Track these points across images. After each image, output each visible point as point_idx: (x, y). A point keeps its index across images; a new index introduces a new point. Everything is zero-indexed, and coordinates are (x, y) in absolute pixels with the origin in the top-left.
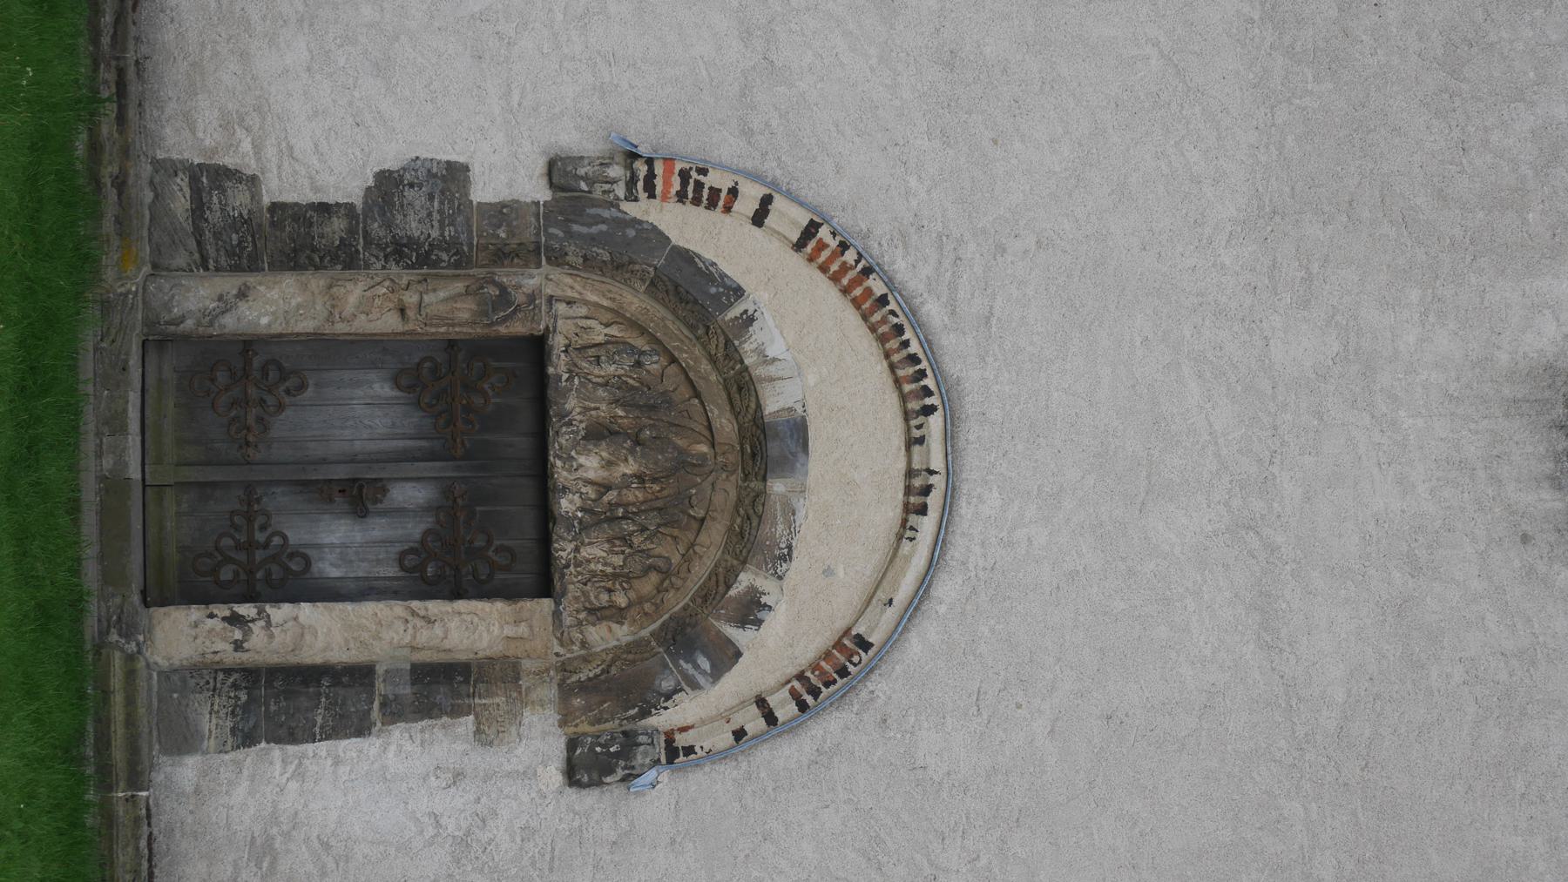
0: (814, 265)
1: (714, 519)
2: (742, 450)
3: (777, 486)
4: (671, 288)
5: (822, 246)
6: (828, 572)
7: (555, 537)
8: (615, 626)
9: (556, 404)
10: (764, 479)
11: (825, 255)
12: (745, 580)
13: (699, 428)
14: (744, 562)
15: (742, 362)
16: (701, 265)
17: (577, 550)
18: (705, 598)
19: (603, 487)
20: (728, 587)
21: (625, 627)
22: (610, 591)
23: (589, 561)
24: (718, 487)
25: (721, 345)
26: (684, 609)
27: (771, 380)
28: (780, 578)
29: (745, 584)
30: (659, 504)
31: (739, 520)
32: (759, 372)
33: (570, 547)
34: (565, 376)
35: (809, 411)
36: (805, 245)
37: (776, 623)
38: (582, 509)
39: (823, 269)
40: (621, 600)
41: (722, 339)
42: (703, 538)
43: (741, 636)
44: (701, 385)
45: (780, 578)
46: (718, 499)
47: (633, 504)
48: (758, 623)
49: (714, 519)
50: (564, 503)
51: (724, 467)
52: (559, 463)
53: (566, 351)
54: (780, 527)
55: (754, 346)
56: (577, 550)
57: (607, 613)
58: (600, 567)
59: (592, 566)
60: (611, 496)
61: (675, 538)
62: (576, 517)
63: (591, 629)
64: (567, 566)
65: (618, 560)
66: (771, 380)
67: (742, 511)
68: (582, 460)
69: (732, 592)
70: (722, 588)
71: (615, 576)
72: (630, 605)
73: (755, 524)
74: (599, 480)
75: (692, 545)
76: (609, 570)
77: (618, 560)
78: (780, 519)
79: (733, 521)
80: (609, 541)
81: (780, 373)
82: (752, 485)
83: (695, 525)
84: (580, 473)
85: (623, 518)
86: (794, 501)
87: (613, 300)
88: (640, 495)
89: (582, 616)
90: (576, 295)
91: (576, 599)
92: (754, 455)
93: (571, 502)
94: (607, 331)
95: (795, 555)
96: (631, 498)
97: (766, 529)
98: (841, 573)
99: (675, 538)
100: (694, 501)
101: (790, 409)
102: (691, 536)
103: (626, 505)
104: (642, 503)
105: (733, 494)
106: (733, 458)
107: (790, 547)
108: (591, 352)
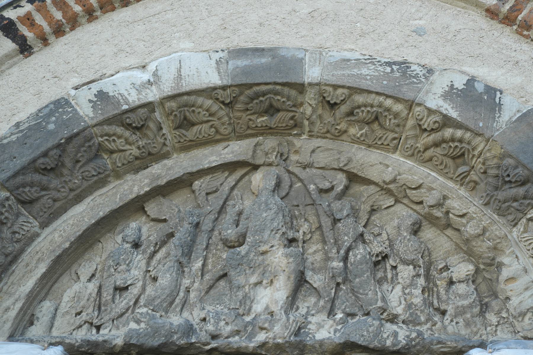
0: (52, 39)
1: (350, 161)
2: (267, 131)
3: (312, 73)
4: (37, 177)
5: (28, 19)
6: (419, 32)
7: (376, 344)
8: (505, 273)
9: (172, 333)
10: (301, 88)
11: (39, 19)
12: (434, 101)
13: (231, 181)
14: (411, 105)
15: (149, 106)
16: (14, 138)
17: (393, 319)
18: (459, 157)
19: (300, 282)
20: (447, 122)
21: (506, 260)
22: (451, 283)
23: (409, 306)
24: (305, 158)
25: (127, 134)
26: (474, 186)
27: (179, 76)
28: (430, 71)
29: (441, 102)
30: (326, 222)
31: (353, 131)
32: (167, 87)
33: (390, 327)
34: (133, 325)
35: (223, 46)
36: (24, 39)
37: (489, 74)
38: (331, 313)
39: (59, 31)
40: (462, 269)
41: (119, 130)
42: (373, 174)
43: (511, 108)
44: (177, 172)
45: (430, 71)
46: (321, 159)
47: (326, 253)
48: (491, 91)
49: (350, 161)
50: (322, 335)
51: (284, 157)
52: (261, 337)
53: (98, 328)
54: (364, 71)
55: (134, 93)
56: (393, 319)
57: (483, 287)
58: (418, 292)
59: (417, 300)
60: (316, 280)
61: (373, 211)
62: (343, 322)
63: (514, 302)
64: (420, 334)
65: (406, 272)
66: (179, 76)
67: (343, 126)
68: (258, 308)
69: (454, 114)
70: (448, 132)
71: (428, 277)
72: (470, 255)
73: (360, 99)
74: (290, 285)
75: (385, 189)
76: (421, 281)
77: (406, 272)
78: (356, 71)
79: (356, 141)
80: (380, 282)
81: (173, 70)
82: (309, 111)
83: (357, 188)
84: (276, 308)
85: (345, 259)
86: (332, 60)
87: (39, 260)
88: (313, 248)
89: (492, 318)
90: (19, 305)
91: (468, 324)
92: (272, 110)
93: (320, 326)
94: (84, 278)
95: (400, 59)
96: (319, 257)
97: (364, 84)
98: (422, 22)
99: (373, 211)
100: (327, 185)
101: (218, 62)
102: (372, 189)
103: (327, 259)
104: (324, 242)
105: (317, 142)
106: (270, 143)
107: (389, 64)
108: (107, 295)
